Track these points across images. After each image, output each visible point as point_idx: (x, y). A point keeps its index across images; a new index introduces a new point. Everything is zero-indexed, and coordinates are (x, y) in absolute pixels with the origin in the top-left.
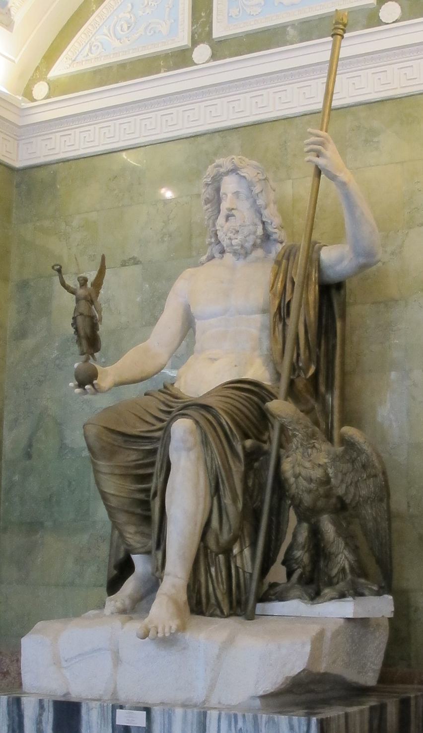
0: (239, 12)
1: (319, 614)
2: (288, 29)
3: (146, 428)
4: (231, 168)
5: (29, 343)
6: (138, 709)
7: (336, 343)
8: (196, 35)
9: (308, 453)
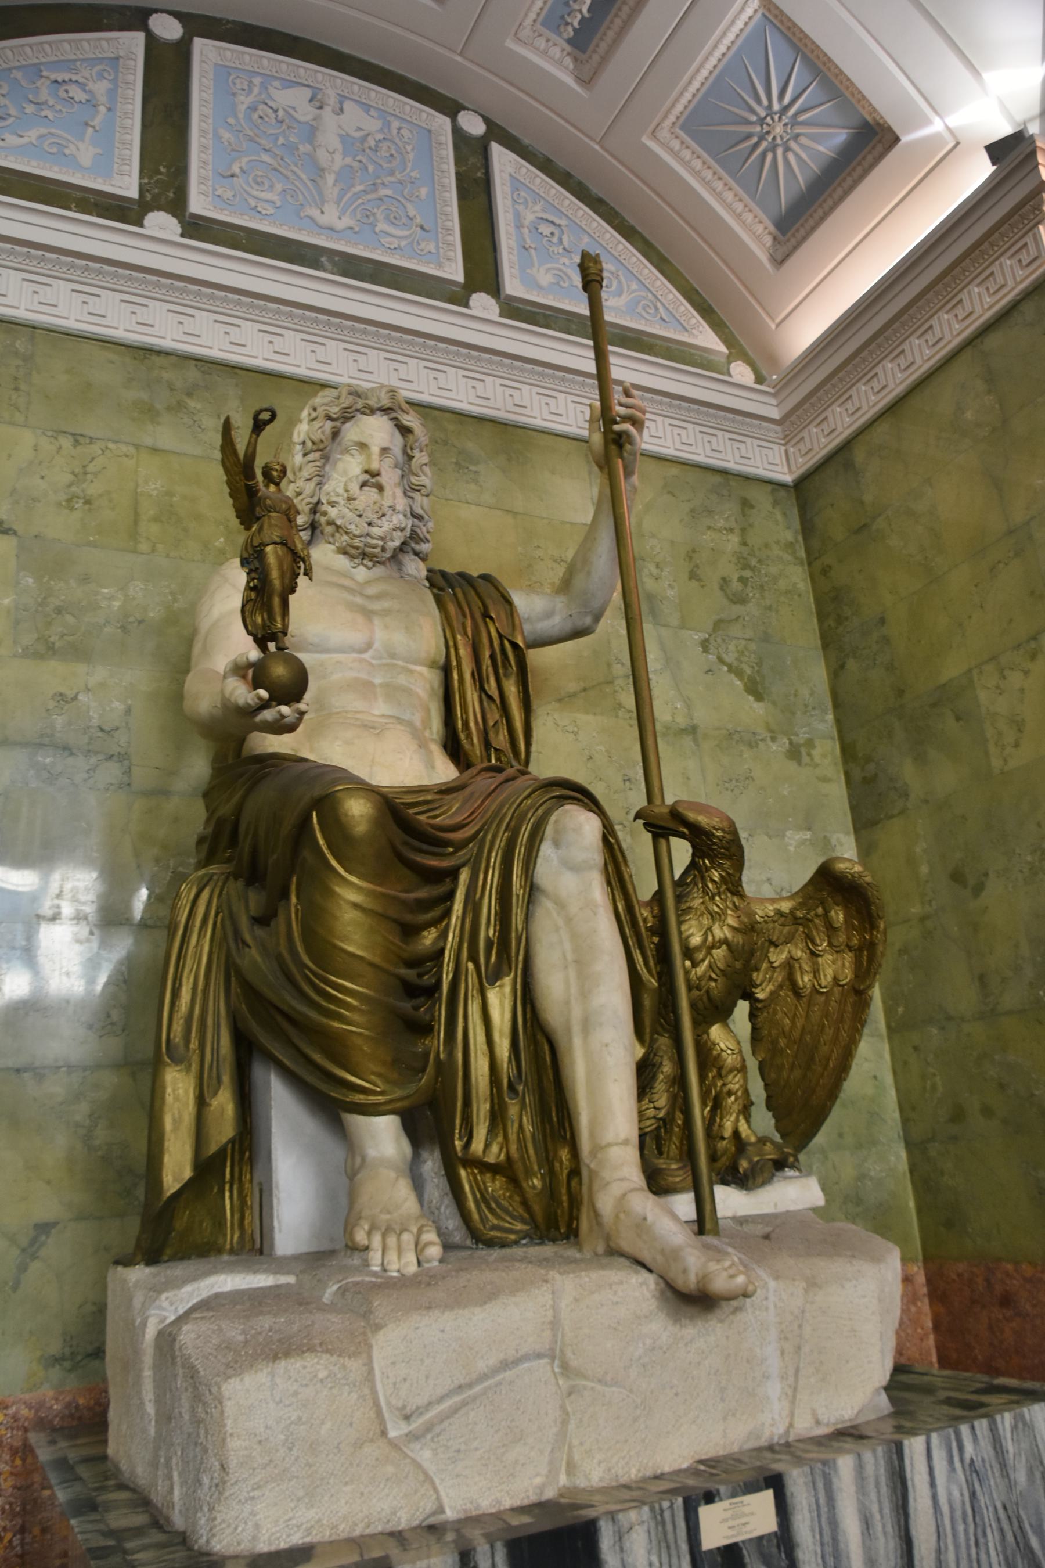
2: (323, 259)
4: (389, 405)
6: (751, 1488)
8: (148, 197)
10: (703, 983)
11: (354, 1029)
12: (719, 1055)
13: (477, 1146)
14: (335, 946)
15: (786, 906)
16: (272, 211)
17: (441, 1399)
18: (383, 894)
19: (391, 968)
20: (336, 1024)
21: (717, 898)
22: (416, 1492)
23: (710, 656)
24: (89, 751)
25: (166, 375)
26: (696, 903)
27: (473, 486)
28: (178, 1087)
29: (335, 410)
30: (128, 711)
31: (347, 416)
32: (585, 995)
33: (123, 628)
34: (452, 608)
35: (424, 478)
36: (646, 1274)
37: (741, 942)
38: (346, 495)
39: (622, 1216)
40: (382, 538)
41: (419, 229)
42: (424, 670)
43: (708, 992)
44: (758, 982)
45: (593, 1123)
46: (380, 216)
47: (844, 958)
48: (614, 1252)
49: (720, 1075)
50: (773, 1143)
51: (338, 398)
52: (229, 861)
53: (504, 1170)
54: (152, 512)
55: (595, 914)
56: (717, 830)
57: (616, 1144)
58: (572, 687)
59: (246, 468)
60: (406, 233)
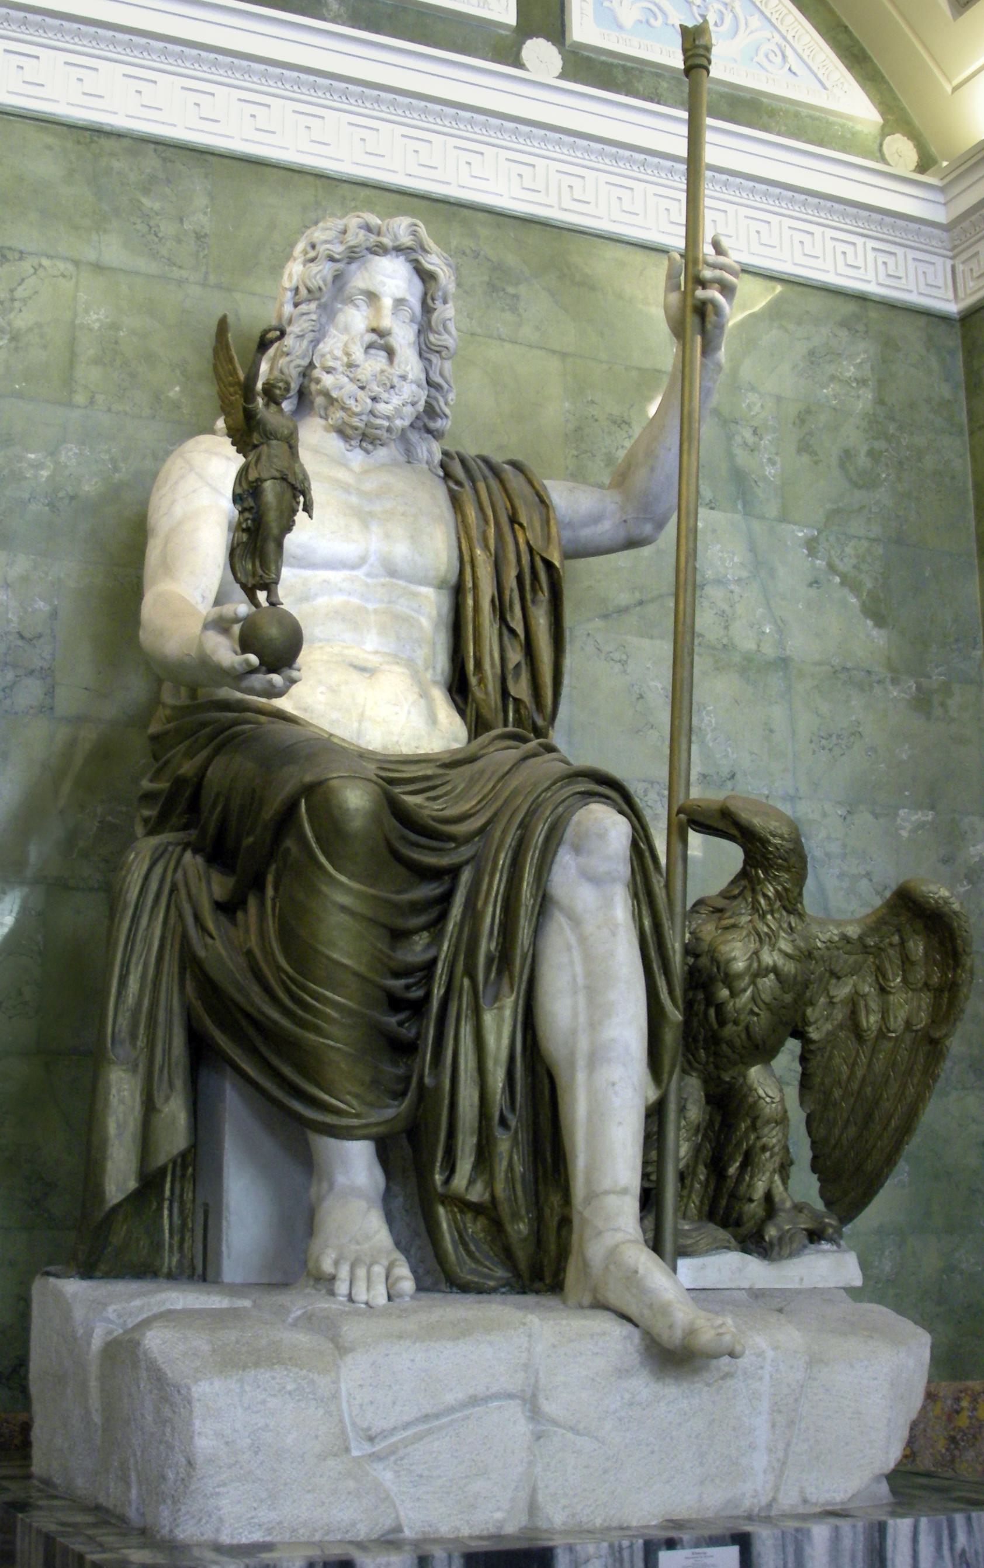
1: (802, 1279)
6: (715, 1541)
9: (790, 924)
10: (742, 1017)
11: (332, 1043)
12: (755, 1103)
13: (460, 1181)
14: (316, 951)
15: (853, 931)
17: (406, 1426)
18: (375, 897)
19: (377, 979)
20: (312, 1037)
21: (769, 917)
22: (376, 1507)
23: (818, 562)
24: (6, 664)
25: (116, 165)
26: (744, 919)
27: (508, 316)
28: (122, 1091)
29: (338, 249)
30: (54, 614)
31: (353, 256)
32: (594, 1026)
33: (52, 505)
34: (471, 513)
35: (446, 336)
36: (629, 1327)
37: (793, 971)
38: (345, 359)
39: (612, 1267)
40: (388, 418)
42: (428, 592)
43: (747, 1028)
44: (812, 1020)
45: (590, 1169)
47: (920, 999)
48: (600, 1305)
49: (754, 1127)
50: (812, 1210)
51: (345, 232)
52: (185, 828)
53: (487, 1211)
54: (91, 352)
55: (614, 934)
56: (774, 836)
57: (615, 1192)
58: (624, 598)
59: (247, 389)
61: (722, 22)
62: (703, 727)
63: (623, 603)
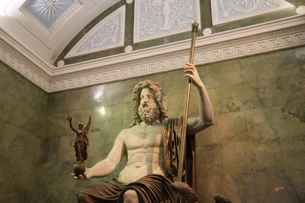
0: (144, 34)
2: (165, 39)
3: (109, 196)
5: (48, 165)
7: (192, 161)
8: (126, 43)
16: (153, 33)
23: (285, 113)
41: (189, 19)
46: (179, 20)
58: (233, 135)
60: (186, 22)
61: (249, 5)
62: (256, 159)
63: (233, 136)
